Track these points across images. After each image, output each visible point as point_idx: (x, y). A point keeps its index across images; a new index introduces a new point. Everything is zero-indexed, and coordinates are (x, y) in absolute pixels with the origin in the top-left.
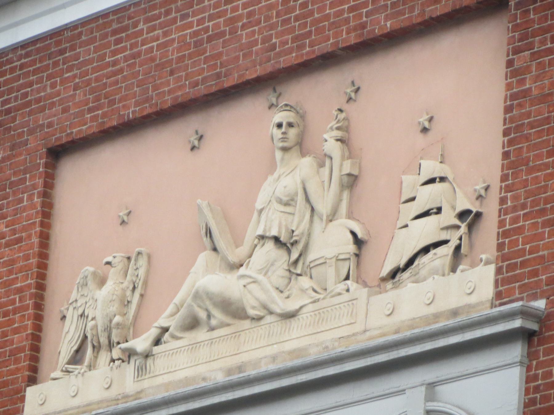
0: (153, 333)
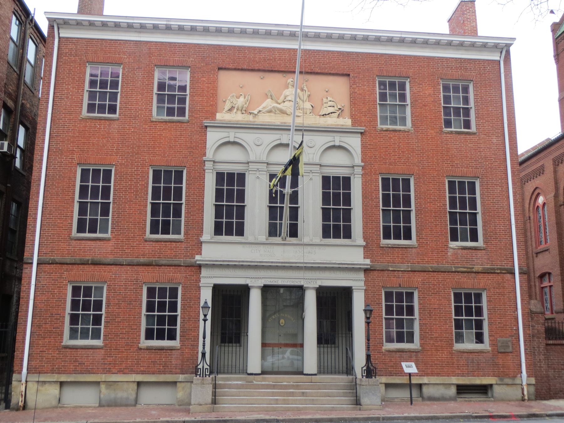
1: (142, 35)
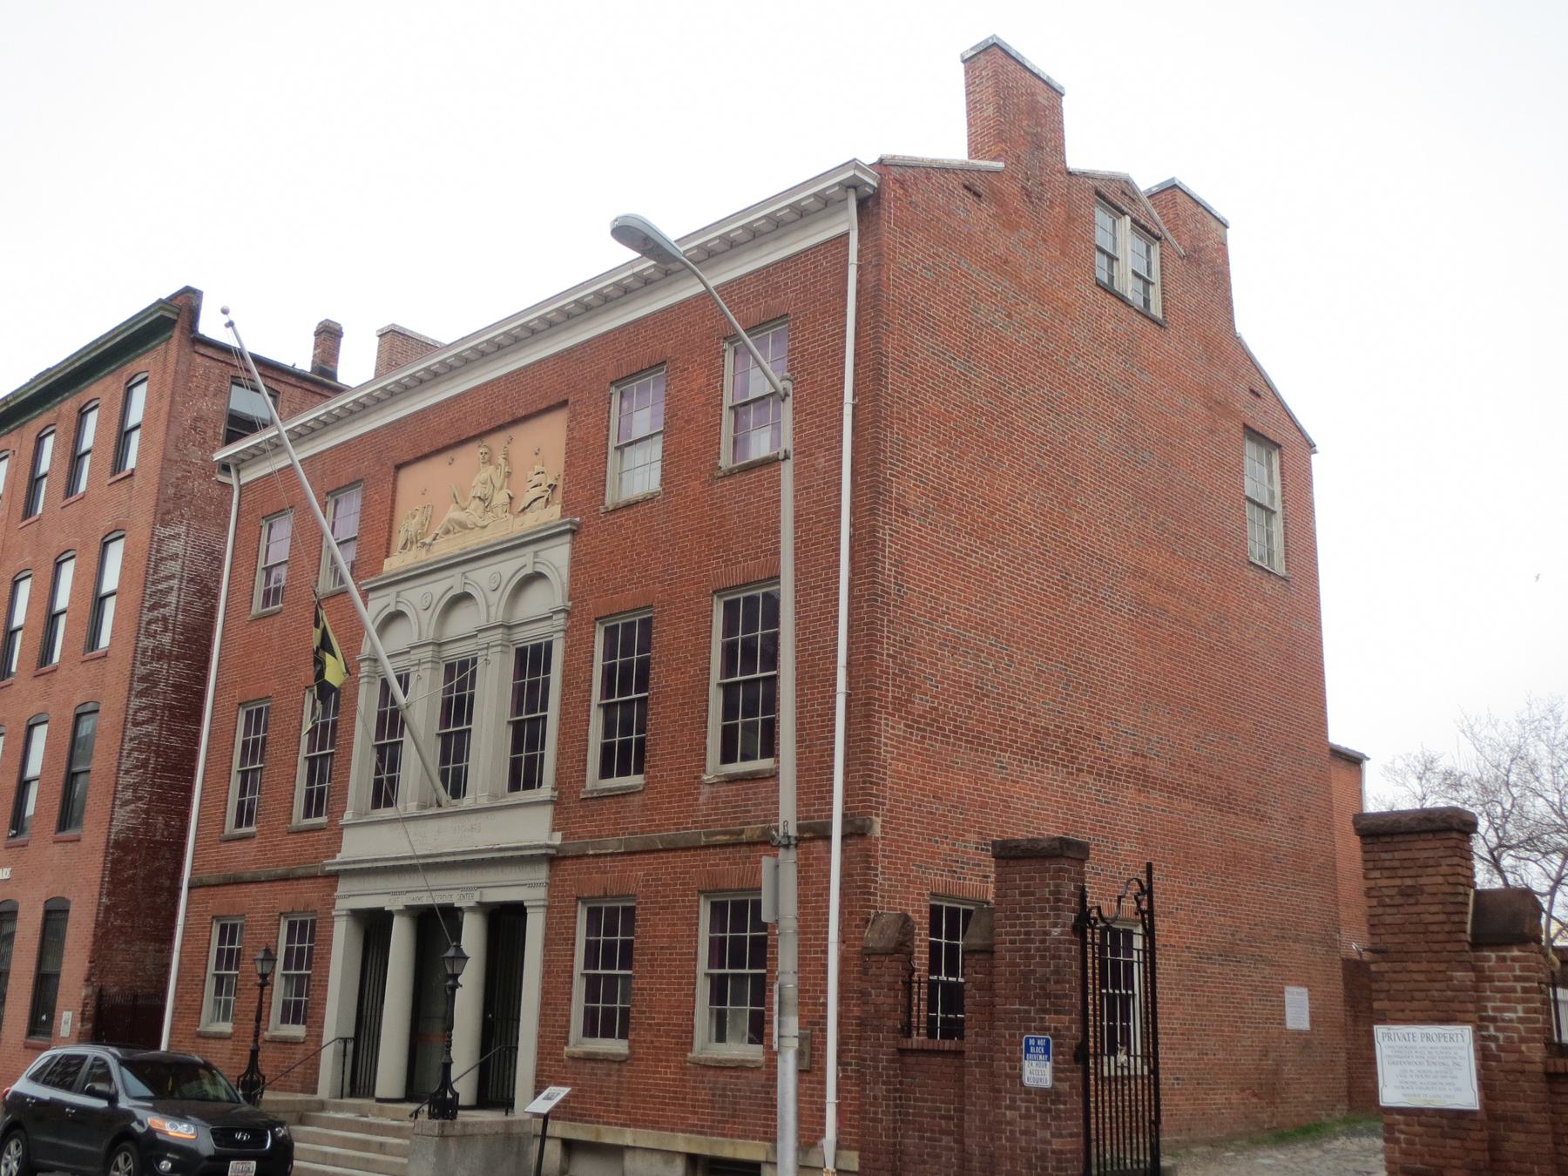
0: (433, 536)
1: (317, 442)
